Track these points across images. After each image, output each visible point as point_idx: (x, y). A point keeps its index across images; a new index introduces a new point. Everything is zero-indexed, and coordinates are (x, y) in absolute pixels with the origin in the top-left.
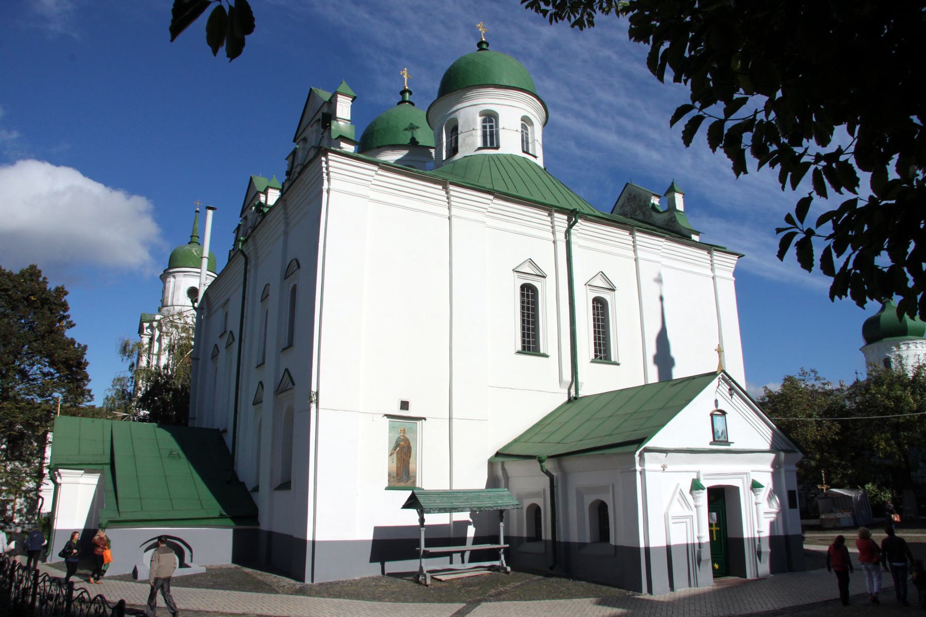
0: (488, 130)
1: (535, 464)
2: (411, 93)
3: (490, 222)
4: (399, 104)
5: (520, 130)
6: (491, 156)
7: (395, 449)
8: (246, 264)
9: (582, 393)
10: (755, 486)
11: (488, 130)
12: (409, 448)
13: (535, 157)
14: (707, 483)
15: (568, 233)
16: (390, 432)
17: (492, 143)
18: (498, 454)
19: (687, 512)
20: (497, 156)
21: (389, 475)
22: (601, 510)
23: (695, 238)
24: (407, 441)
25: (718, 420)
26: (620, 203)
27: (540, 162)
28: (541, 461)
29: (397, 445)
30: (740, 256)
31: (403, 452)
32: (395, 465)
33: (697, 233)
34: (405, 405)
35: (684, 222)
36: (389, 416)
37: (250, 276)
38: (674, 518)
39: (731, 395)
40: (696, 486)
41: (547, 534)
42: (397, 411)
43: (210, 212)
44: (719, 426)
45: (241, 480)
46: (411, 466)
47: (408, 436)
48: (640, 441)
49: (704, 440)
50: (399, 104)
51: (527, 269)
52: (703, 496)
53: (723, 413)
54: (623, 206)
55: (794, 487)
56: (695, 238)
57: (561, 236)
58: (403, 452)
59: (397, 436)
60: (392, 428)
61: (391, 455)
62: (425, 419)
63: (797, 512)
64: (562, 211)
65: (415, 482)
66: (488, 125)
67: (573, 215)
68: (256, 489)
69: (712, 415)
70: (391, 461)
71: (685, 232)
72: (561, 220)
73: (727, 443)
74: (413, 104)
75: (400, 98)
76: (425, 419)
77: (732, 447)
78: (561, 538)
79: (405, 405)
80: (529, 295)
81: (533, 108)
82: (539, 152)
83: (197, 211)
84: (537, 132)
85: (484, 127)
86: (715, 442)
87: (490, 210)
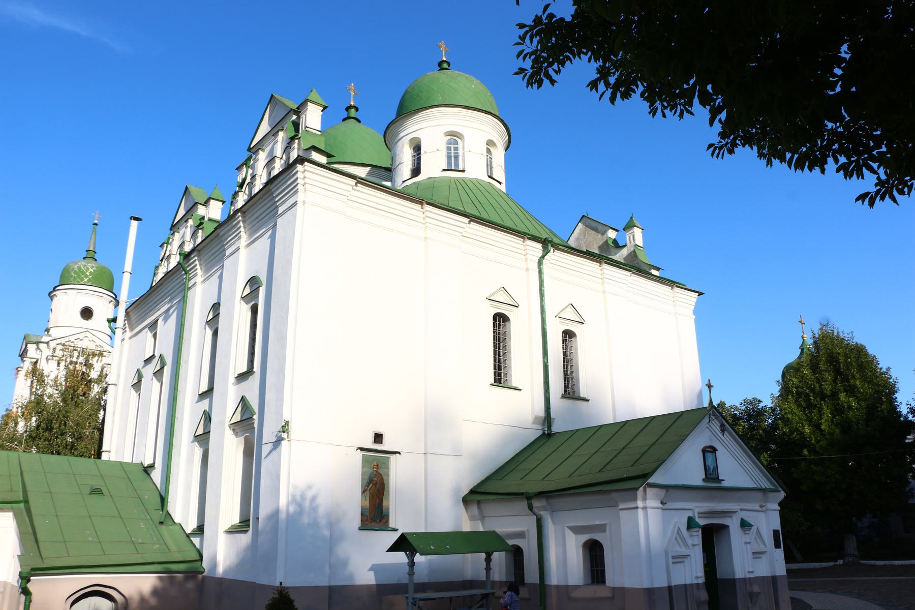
0: (453, 151)
2: (357, 109)
4: (344, 120)
5: (485, 154)
6: (456, 180)
7: (369, 483)
9: (555, 429)
10: (745, 525)
11: (453, 151)
13: (500, 183)
14: (702, 522)
15: (540, 263)
16: (363, 467)
17: (457, 164)
18: (473, 492)
19: (683, 551)
20: (463, 179)
21: (362, 514)
23: (654, 272)
25: (709, 456)
27: (503, 188)
29: (370, 481)
30: (700, 294)
32: (367, 503)
33: (658, 269)
34: (378, 438)
35: (643, 257)
36: (362, 449)
38: (674, 557)
39: (723, 431)
40: (691, 524)
41: (531, 575)
42: (370, 444)
43: (134, 223)
44: (710, 462)
45: (177, 520)
46: (384, 503)
47: (381, 471)
48: (646, 476)
49: (697, 477)
50: (344, 120)
55: (778, 527)
56: (654, 272)
59: (371, 471)
60: (365, 461)
61: (364, 492)
62: (399, 453)
64: (534, 238)
65: (387, 521)
66: (452, 146)
67: (547, 244)
68: (200, 530)
69: (704, 451)
73: (718, 480)
74: (359, 121)
75: (345, 115)
76: (399, 453)
77: (724, 484)
79: (378, 438)
82: (502, 179)
83: (96, 224)
84: (499, 155)
85: (449, 148)
86: (707, 479)
87: (465, 234)
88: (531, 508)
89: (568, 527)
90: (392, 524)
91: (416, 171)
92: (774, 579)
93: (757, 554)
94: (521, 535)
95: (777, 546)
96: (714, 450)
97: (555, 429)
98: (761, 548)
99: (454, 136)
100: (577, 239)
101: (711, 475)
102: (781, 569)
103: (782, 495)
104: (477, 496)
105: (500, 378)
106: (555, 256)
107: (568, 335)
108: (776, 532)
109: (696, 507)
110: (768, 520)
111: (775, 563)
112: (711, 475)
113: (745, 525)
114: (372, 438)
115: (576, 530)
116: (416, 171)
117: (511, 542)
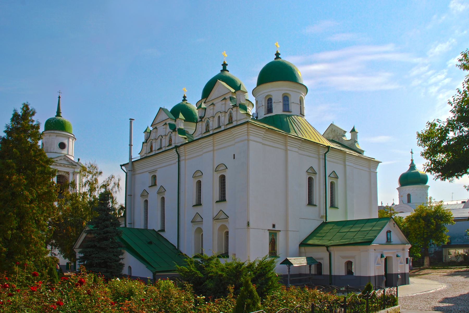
1: (325, 248)
3: (300, 152)
12: (275, 242)
22: (349, 264)
24: (274, 239)
26: (327, 132)
31: (273, 243)
34: (274, 226)
37: (182, 163)
42: (271, 228)
51: (309, 171)
54: (328, 134)
57: (322, 157)
58: (273, 243)
70: (270, 247)
71: (358, 151)
78: (333, 274)
79: (274, 226)
80: (310, 180)
88: (328, 250)
91: (270, 110)
94: (322, 259)
105: (310, 203)
107: (332, 184)
114: (272, 226)
115: (343, 257)
117: (318, 261)
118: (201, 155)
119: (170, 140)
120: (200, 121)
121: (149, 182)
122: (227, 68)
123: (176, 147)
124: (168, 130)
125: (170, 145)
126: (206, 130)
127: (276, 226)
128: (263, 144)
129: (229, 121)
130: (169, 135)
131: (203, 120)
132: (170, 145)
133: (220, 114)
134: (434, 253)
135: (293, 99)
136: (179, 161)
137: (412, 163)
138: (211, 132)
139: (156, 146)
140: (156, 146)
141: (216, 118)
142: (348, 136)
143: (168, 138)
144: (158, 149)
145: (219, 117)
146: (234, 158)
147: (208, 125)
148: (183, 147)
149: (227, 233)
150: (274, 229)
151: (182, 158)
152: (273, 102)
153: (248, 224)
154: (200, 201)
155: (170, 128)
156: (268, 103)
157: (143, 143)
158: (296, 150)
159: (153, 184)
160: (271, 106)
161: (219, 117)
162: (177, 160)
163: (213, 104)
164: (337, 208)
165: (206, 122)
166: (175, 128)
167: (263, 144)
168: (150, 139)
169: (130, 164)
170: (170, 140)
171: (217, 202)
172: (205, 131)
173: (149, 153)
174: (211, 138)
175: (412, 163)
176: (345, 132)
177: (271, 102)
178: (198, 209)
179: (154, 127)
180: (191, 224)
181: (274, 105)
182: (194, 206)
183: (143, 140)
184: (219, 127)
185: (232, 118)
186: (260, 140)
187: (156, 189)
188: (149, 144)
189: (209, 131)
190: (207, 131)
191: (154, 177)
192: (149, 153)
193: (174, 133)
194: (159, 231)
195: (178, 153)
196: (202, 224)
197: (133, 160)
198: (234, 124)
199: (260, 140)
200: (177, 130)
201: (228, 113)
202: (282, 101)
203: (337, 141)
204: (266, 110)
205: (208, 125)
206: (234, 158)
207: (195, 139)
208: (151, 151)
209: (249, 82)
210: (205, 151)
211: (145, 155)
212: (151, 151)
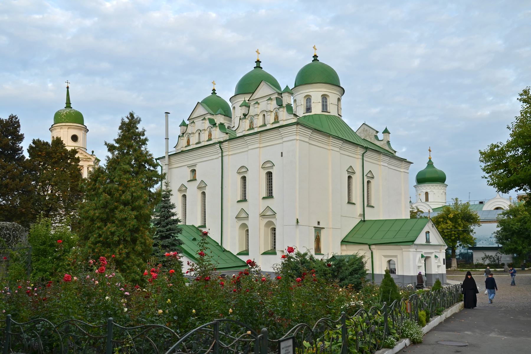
1: (368, 246)
8: (222, 153)
10: (436, 257)
17: (327, 109)
24: (319, 236)
28: (369, 245)
34: (319, 223)
42: (316, 225)
48: (413, 241)
49: (424, 242)
51: (350, 170)
52: (424, 259)
53: (429, 232)
63: (445, 265)
64: (362, 147)
72: (360, 151)
73: (429, 242)
77: (431, 243)
79: (319, 223)
81: (338, 91)
88: (370, 248)
89: (383, 256)
90: (322, 252)
91: (309, 109)
92: (442, 274)
93: (438, 266)
95: (444, 264)
96: (429, 232)
97: (366, 219)
98: (440, 264)
99: (324, 97)
100: (360, 133)
101: (428, 241)
102: (445, 272)
103: (447, 247)
104: (344, 242)
106: (369, 153)
107: (368, 182)
108: (444, 259)
109: (425, 251)
110: (442, 256)
111: (443, 270)
112: (428, 241)
113: (436, 257)
115: (385, 256)
116: (309, 109)
118: (247, 151)
119: (210, 135)
120: (243, 119)
121: (189, 177)
122: (261, 65)
123: (220, 143)
124: (207, 124)
125: (210, 139)
126: (250, 126)
127: (320, 223)
128: (310, 144)
129: (275, 119)
130: (208, 130)
131: (247, 117)
132: (210, 139)
133: (265, 113)
134: (459, 255)
135: (332, 99)
136: (222, 156)
137: (430, 161)
138: (256, 130)
139: (194, 140)
140: (194, 140)
141: (261, 117)
142: (381, 136)
143: (207, 133)
144: (197, 144)
145: (264, 115)
146: (282, 156)
147: (251, 123)
148: (227, 142)
149: (274, 229)
150: (319, 226)
151: (224, 154)
152: (312, 102)
153: (298, 222)
154: (245, 196)
155: (210, 122)
156: (307, 103)
157: (179, 136)
158: (338, 150)
159: (192, 179)
160: (310, 106)
161: (264, 115)
162: (220, 155)
163: (257, 103)
164: (373, 207)
165: (249, 119)
166: (216, 124)
167: (310, 144)
168: (187, 132)
169: (167, 158)
170: (210, 135)
171: (264, 198)
172: (248, 128)
173: (186, 147)
174: (258, 135)
175: (430, 161)
176: (377, 132)
177: (310, 102)
178: (243, 205)
179: (191, 121)
180: (236, 220)
181: (313, 105)
182: (238, 202)
183: (179, 133)
184: (265, 125)
185: (278, 118)
186: (307, 140)
187: (196, 184)
188: (185, 139)
189: (253, 129)
190: (251, 128)
191: (194, 171)
192: (186, 147)
193: (214, 129)
194: (200, 227)
195: (221, 149)
196: (248, 220)
197: (169, 154)
198: (281, 123)
199: (307, 140)
200: (217, 125)
201: (274, 112)
202: (321, 101)
203: (369, 140)
204: (305, 109)
205: (251, 123)
206: (282, 156)
207: (238, 135)
208: (188, 145)
209: (286, 80)
210: (250, 147)
211: (182, 149)
212: (188, 145)
